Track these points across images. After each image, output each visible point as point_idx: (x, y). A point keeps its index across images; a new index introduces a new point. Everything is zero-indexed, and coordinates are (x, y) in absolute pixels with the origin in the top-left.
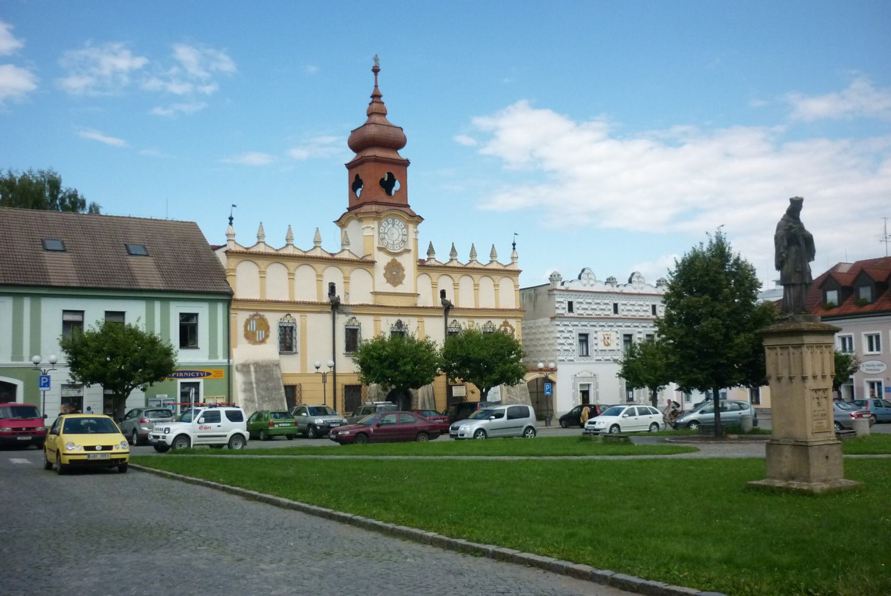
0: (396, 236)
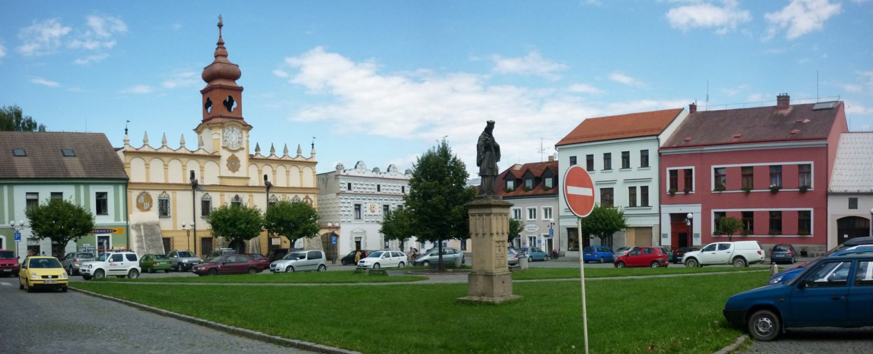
0: (234, 139)
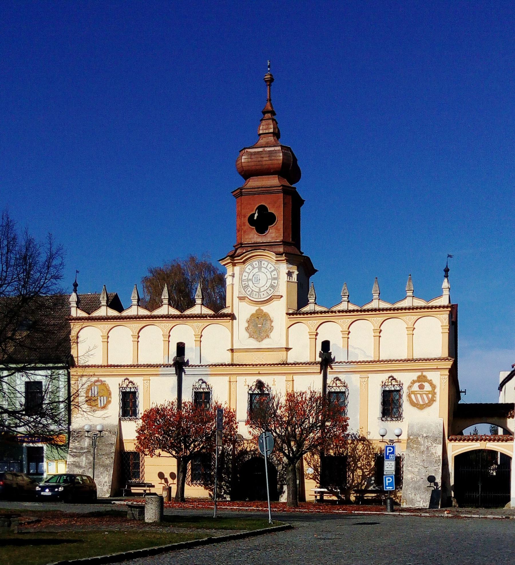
0: (262, 282)
